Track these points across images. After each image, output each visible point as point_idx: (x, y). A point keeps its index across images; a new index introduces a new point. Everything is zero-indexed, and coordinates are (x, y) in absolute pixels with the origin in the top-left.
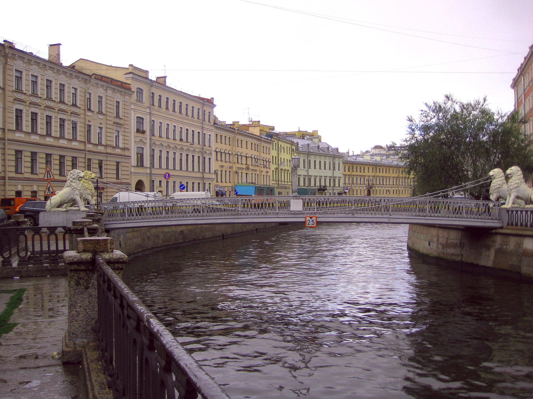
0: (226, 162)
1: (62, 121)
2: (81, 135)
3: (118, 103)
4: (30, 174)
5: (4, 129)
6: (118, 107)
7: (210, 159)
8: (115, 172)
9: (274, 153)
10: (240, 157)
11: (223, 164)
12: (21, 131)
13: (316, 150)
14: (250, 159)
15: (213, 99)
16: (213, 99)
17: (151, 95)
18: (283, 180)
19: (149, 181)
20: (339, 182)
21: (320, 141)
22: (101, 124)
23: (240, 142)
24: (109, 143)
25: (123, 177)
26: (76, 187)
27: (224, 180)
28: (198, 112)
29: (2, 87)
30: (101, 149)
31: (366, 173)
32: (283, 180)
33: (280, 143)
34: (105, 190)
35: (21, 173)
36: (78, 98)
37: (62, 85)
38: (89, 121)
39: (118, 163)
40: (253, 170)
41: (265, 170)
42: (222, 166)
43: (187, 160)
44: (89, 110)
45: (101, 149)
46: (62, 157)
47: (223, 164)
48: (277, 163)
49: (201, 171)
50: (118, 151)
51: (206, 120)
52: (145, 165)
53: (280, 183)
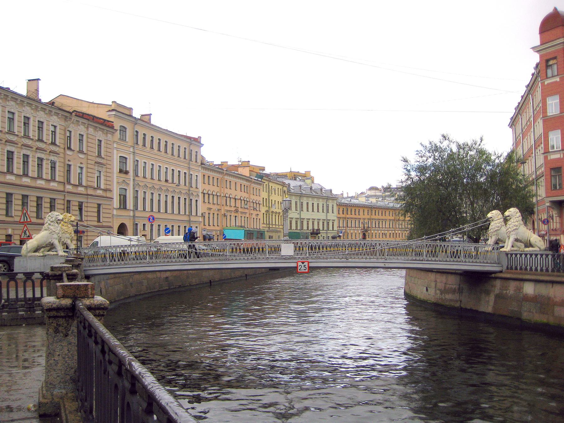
0: (214, 204)
1: (41, 160)
2: (59, 175)
3: (100, 141)
4: (4, 217)
6: (100, 146)
7: (196, 201)
8: (96, 214)
9: (264, 195)
10: (228, 199)
11: (211, 206)
13: (308, 192)
14: (240, 201)
15: (200, 137)
16: (200, 137)
17: (135, 133)
18: (274, 223)
19: (132, 224)
20: (333, 225)
21: (313, 182)
22: (81, 163)
23: (228, 183)
24: (90, 184)
27: (211, 224)
28: (185, 152)
30: (81, 190)
31: (361, 216)
32: (274, 223)
33: (271, 184)
34: (86, 234)
36: (58, 136)
37: (41, 123)
39: (99, 205)
40: (242, 213)
41: (255, 213)
42: (210, 209)
43: (173, 202)
44: (69, 148)
45: (81, 190)
46: (39, 199)
47: (211, 206)
48: (268, 205)
49: (187, 214)
50: (99, 192)
51: (192, 160)
52: (128, 208)
53: (271, 226)
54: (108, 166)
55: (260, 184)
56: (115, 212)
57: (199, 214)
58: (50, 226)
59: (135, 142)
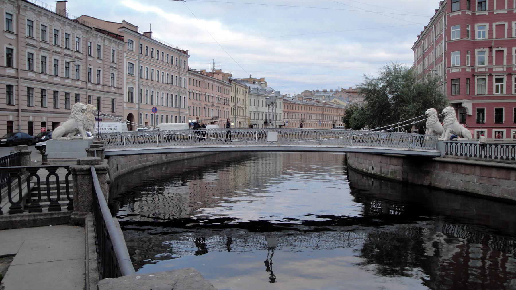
0: (197, 100)
5: (17, 69)
10: (207, 97)
11: (195, 101)
12: (32, 71)
15: (187, 50)
16: (187, 50)
17: (140, 46)
21: (266, 86)
22: (99, 67)
23: (207, 85)
24: (106, 83)
25: (117, 110)
29: (15, 33)
30: (99, 87)
31: (300, 111)
33: (237, 87)
35: (33, 107)
39: (113, 100)
40: (217, 107)
41: (225, 107)
42: (194, 103)
44: (90, 56)
47: (195, 101)
50: (113, 90)
52: (134, 102)
54: (120, 70)
55: (230, 86)
56: (125, 105)
57: (187, 107)
59: (140, 52)
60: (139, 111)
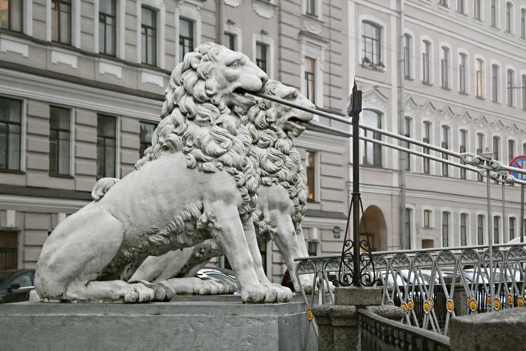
4: (46, 175)
19: (396, 211)
22: (263, 33)
26: (213, 147)
35: (19, 172)
38: (230, 22)
54: (335, 46)
58: (192, 128)
60: (402, 197)
